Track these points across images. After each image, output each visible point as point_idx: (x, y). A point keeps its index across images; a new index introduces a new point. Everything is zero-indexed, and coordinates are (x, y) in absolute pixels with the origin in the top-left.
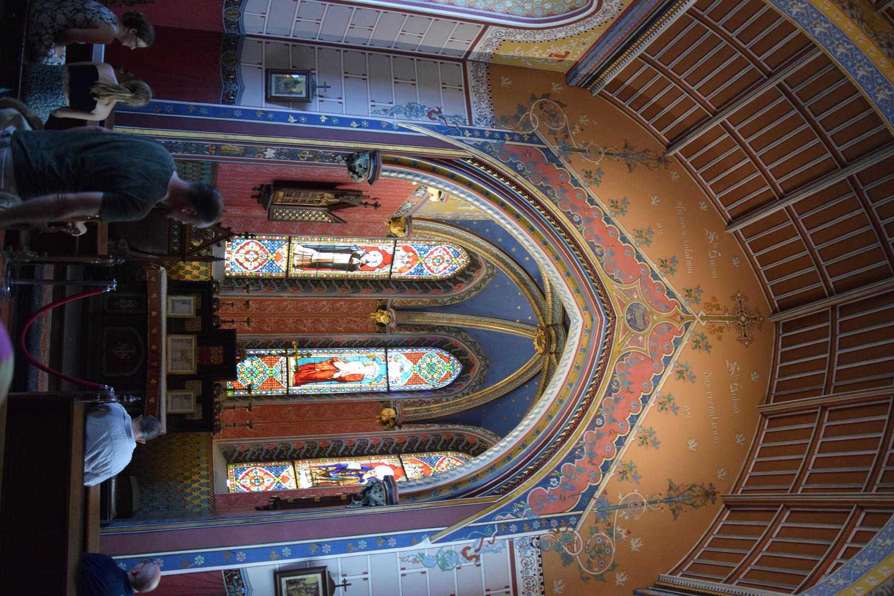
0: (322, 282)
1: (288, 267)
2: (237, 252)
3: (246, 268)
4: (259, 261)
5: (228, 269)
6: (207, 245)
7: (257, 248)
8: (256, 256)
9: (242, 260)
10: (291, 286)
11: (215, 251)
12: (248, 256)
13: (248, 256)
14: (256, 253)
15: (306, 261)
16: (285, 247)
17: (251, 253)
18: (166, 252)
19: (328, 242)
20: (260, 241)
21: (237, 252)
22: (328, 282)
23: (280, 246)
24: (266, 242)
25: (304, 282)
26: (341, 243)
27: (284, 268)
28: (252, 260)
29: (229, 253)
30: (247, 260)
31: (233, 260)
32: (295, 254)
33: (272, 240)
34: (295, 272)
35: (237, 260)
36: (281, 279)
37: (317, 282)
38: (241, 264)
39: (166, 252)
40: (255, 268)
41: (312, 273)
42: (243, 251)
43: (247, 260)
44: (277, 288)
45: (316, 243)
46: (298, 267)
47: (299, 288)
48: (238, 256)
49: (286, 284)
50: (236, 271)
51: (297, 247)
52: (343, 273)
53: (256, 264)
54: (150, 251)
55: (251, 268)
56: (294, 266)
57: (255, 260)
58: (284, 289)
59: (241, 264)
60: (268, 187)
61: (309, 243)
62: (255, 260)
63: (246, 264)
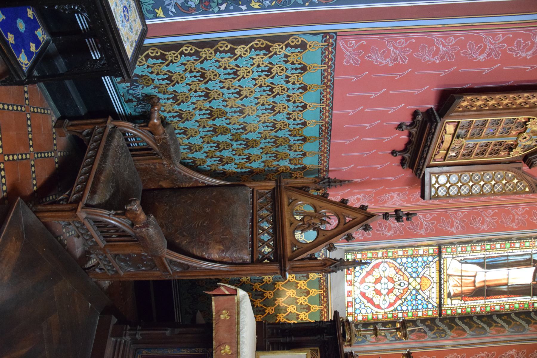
0: (495, 317)
1: (440, 298)
2: (363, 281)
3: (378, 306)
4: (396, 291)
5: (350, 310)
6: (326, 240)
7: (391, 272)
8: (390, 286)
9: (370, 293)
10: (451, 328)
11: (341, 250)
12: (378, 286)
13: (378, 286)
14: (391, 279)
15: (467, 285)
16: (434, 267)
17: (384, 280)
18: (247, 258)
19: (497, 251)
20: (395, 259)
21: (363, 281)
22: (506, 317)
23: (426, 265)
24: (404, 260)
25: (468, 319)
26: (517, 251)
27: (435, 301)
28: (384, 292)
29: (351, 283)
30: (378, 292)
31: (357, 294)
32: (449, 275)
33: (412, 256)
34: (453, 306)
35: (363, 294)
36: (433, 319)
37: (489, 319)
38: (370, 301)
39: (247, 258)
40: (391, 305)
41: (479, 305)
42: (371, 279)
43: (378, 292)
44: (430, 334)
45: (479, 253)
46: (456, 296)
47: (464, 330)
48: (363, 288)
49: (443, 326)
50: (363, 311)
51: (452, 265)
52: (526, 299)
53: (392, 298)
54: (215, 256)
55: (384, 308)
56: (449, 295)
57: (390, 291)
58: (441, 334)
59: (370, 301)
60: (429, 113)
61: (467, 256)
62: (390, 291)
63: (377, 300)
